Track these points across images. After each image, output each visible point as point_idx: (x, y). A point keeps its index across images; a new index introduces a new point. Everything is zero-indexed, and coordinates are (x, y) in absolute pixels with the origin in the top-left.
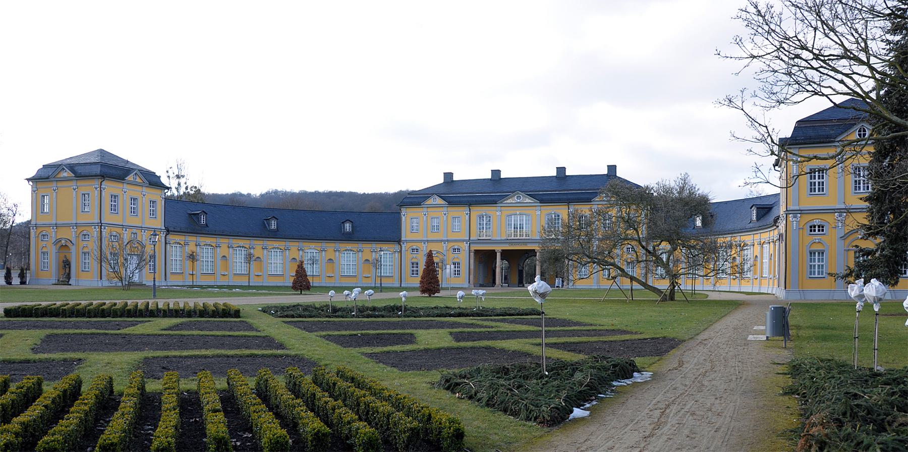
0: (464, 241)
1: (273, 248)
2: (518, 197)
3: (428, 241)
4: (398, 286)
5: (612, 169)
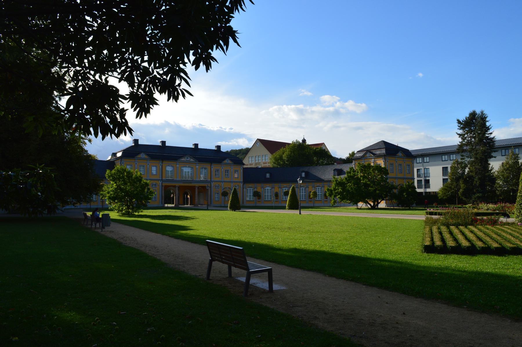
0: (159, 180)
1: (249, 188)
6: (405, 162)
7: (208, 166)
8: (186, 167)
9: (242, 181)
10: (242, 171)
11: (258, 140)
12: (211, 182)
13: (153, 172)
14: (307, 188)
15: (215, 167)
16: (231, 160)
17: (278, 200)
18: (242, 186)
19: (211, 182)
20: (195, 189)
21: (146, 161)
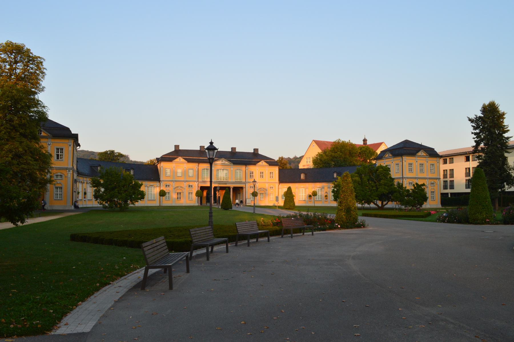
2: (222, 161)
3: (176, 181)
4: (159, 205)
6: (427, 162)
7: (243, 168)
11: (313, 141)
12: (245, 183)
13: (189, 174)
14: (323, 189)
17: (311, 200)
19: (245, 183)
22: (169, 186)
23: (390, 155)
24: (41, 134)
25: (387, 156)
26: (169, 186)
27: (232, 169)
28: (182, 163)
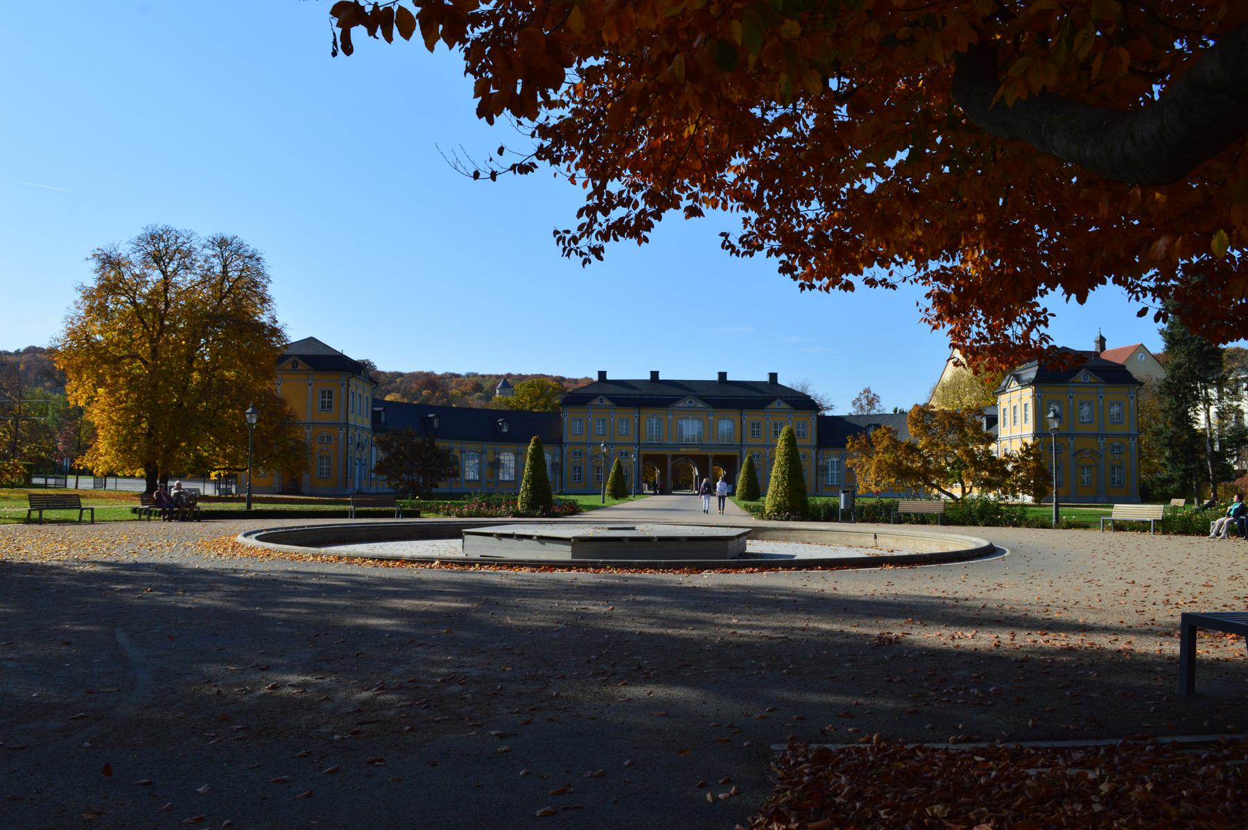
5: (773, 376)
6: (1101, 397)
7: (735, 414)
8: (688, 419)
9: (814, 443)
10: (814, 423)
15: (751, 417)
16: (787, 402)
18: (814, 455)
20: (736, 459)
21: (608, 410)
22: (580, 454)
23: (1017, 384)
24: (297, 366)
25: (1012, 385)
26: (580, 454)
27: (711, 418)
28: (606, 407)
